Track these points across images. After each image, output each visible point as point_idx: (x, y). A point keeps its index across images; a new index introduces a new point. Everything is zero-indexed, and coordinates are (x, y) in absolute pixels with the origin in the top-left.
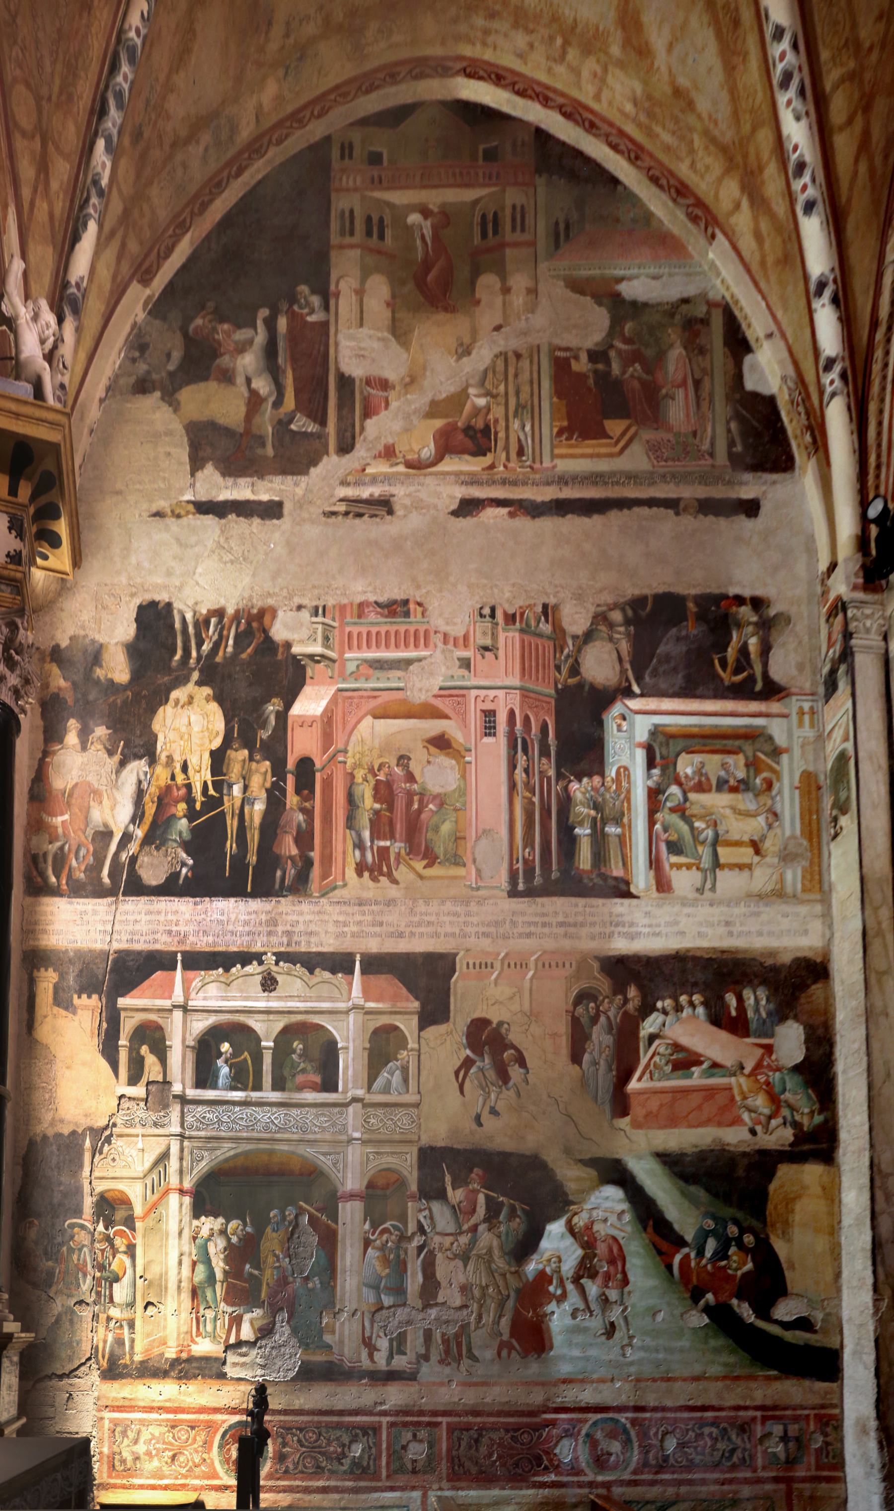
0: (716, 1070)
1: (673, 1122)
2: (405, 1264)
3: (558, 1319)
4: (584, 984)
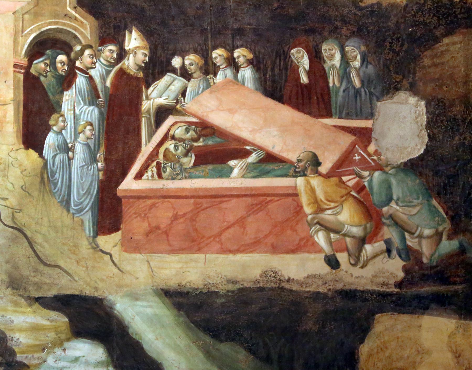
0: (271, 166)
1: (194, 243)
4: (47, 25)
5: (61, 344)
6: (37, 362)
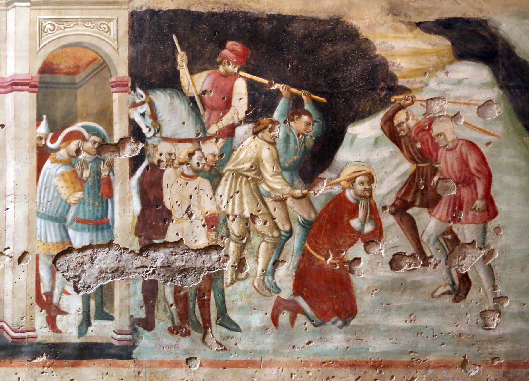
2: (109, 183)
5: (444, 68)
6: (419, 85)
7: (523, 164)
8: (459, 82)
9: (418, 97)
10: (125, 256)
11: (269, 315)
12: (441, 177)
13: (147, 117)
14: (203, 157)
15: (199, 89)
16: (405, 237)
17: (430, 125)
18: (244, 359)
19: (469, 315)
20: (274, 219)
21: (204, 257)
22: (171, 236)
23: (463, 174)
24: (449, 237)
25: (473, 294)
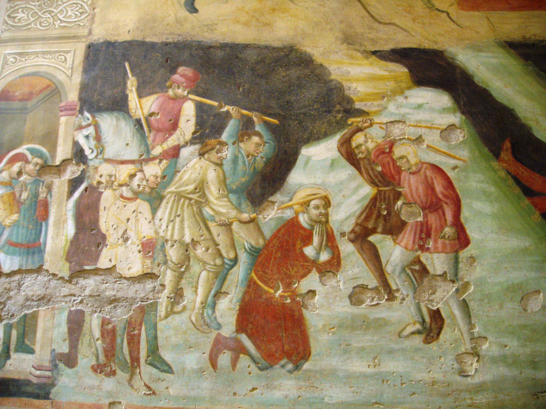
3: (325, 302)
6: (377, 109)
7: (493, 189)
8: (420, 107)
9: (376, 120)
10: (54, 283)
11: (207, 356)
12: (405, 202)
13: (91, 139)
14: (144, 178)
15: (146, 112)
16: (367, 267)
17: (391, 148)
18: (176, 406)
19: (442, 359)
20: (218, 245)
21: (137, 286)
22: (103, 263)
23: (429, 199)
24: (417, 267)
25: (446, 334)
